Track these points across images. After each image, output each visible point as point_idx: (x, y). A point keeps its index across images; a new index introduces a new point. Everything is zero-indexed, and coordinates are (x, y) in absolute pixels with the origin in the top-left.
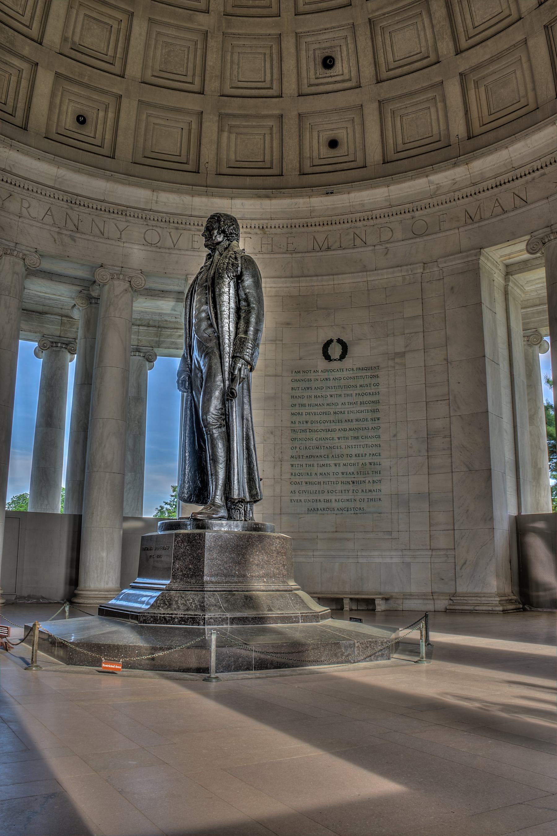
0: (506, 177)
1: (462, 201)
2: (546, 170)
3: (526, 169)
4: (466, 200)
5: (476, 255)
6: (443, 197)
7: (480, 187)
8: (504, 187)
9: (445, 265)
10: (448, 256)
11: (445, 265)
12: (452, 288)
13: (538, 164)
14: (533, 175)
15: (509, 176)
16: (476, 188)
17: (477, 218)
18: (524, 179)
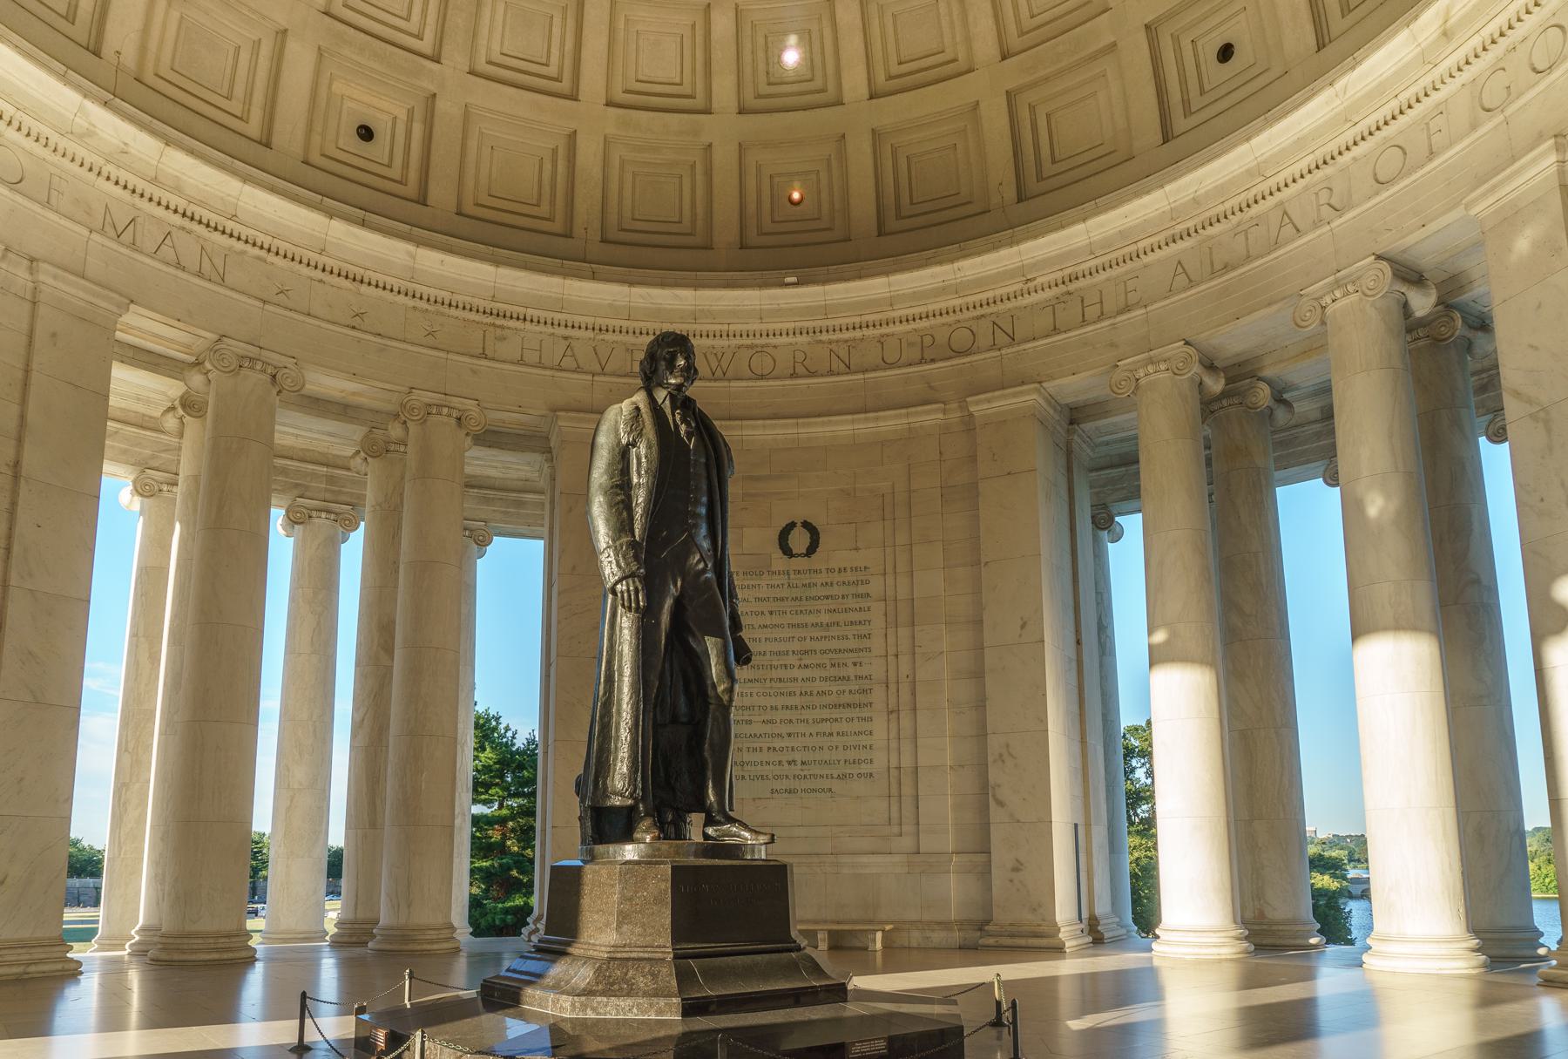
0: (207, 215)
1: (109, 186)
2: (271, 258)
3: (245, 232)
4: (118, 191)
5: (119, 306)
6: (81, 152)
7: (157, 193)
8: (194, 226)
9: (50, 281)
10: (66, 270)
11: (50, 281)
12: (54, 335)
13: (267, 241)
14: (248, 248)
15: (214, 219)
16: (150, 190)
17: (127, 237)
18: (233, 242)
